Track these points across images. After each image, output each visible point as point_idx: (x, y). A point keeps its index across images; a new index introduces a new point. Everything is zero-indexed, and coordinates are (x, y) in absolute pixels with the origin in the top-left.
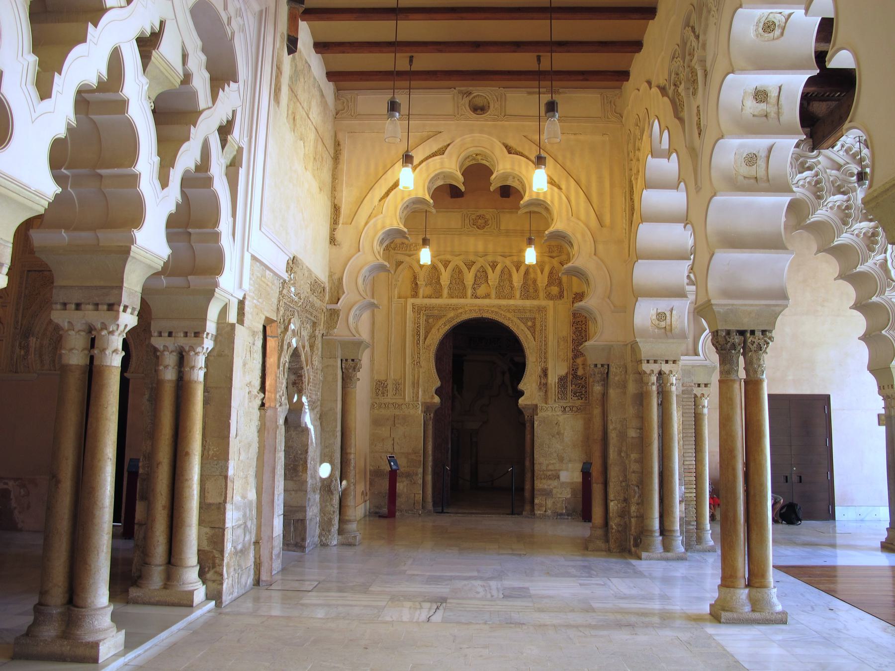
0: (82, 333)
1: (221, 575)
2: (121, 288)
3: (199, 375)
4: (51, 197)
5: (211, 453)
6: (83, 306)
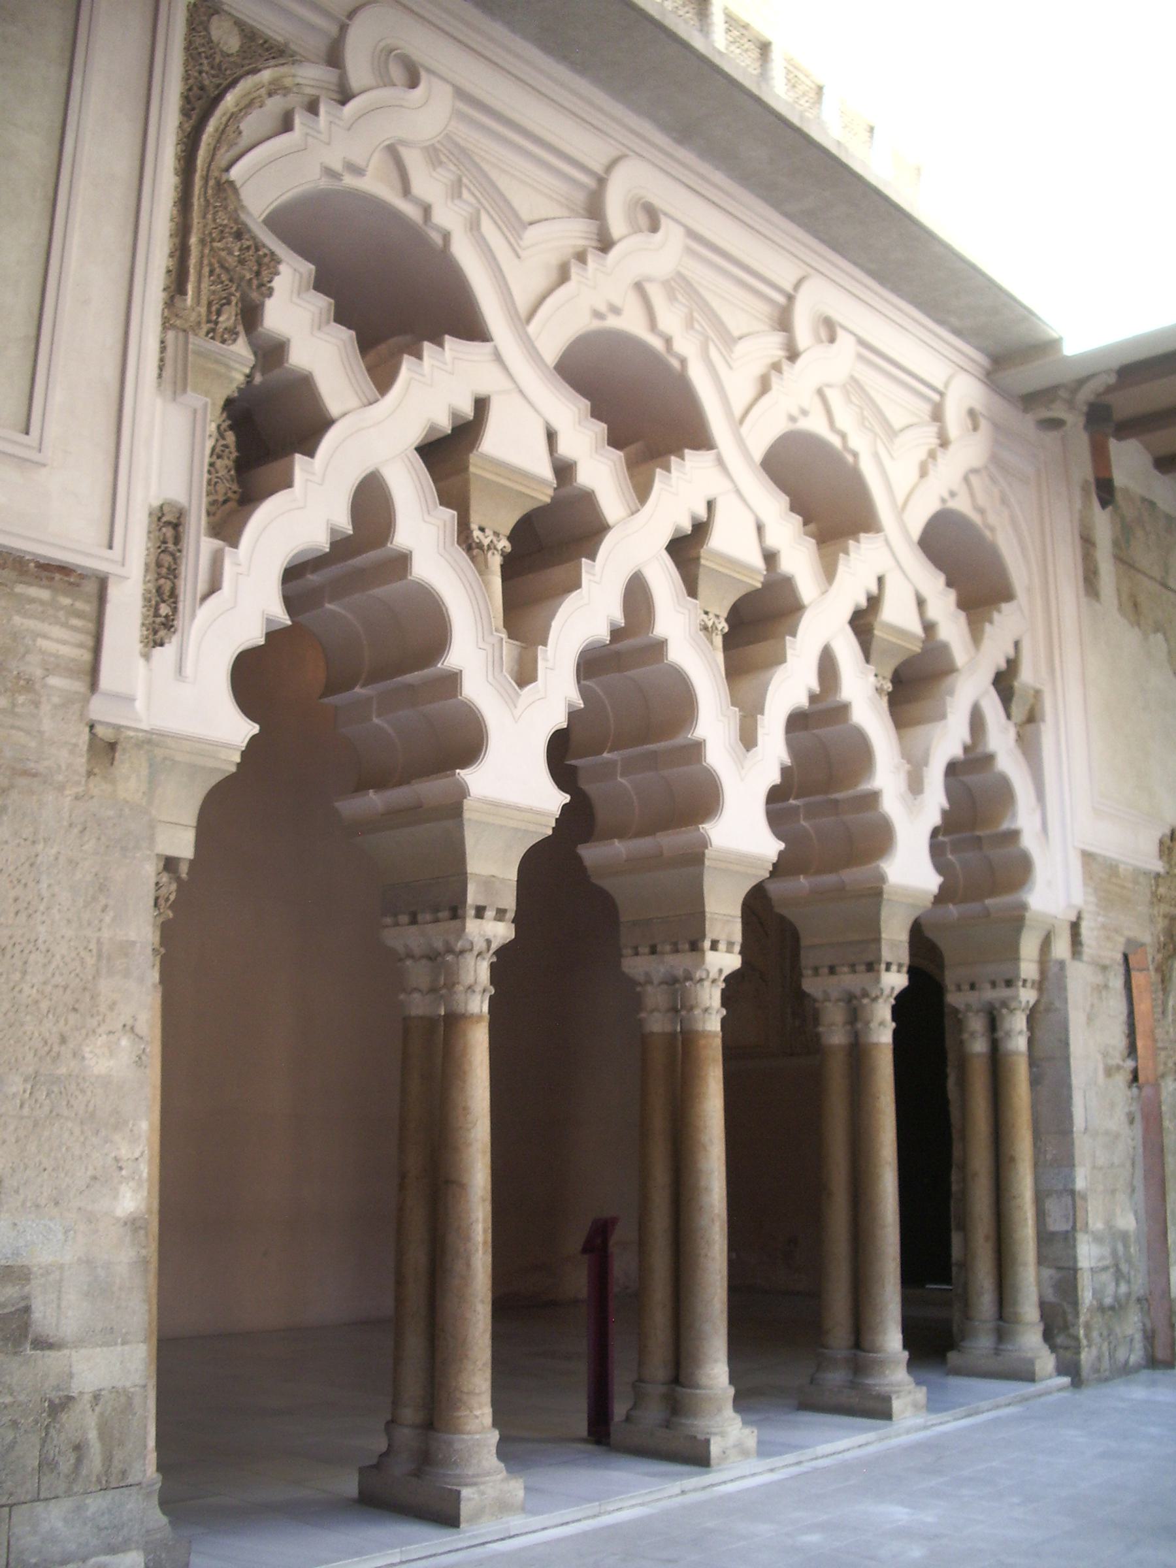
0: (841, 1004)
1: (1076, 1339)
2: (878, 940)
3: (1019, 1043)
4: (774, 857)
5: (1049, 1157)
6: (838, 968)
